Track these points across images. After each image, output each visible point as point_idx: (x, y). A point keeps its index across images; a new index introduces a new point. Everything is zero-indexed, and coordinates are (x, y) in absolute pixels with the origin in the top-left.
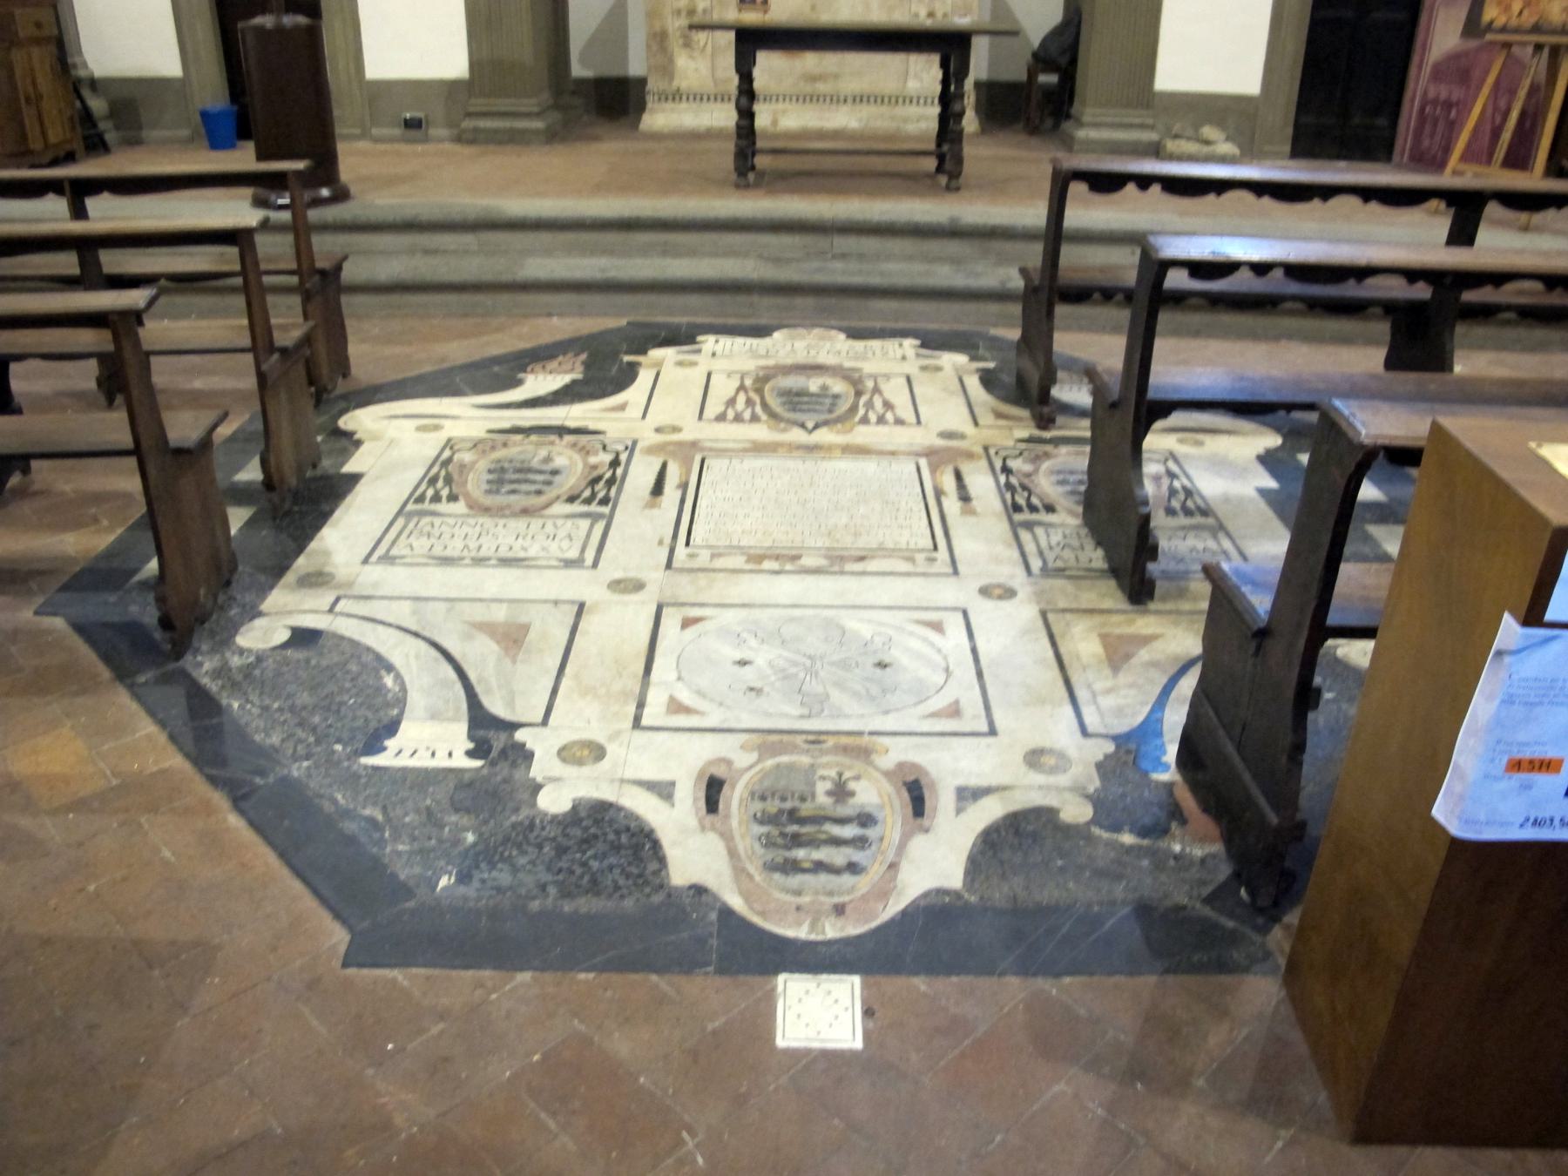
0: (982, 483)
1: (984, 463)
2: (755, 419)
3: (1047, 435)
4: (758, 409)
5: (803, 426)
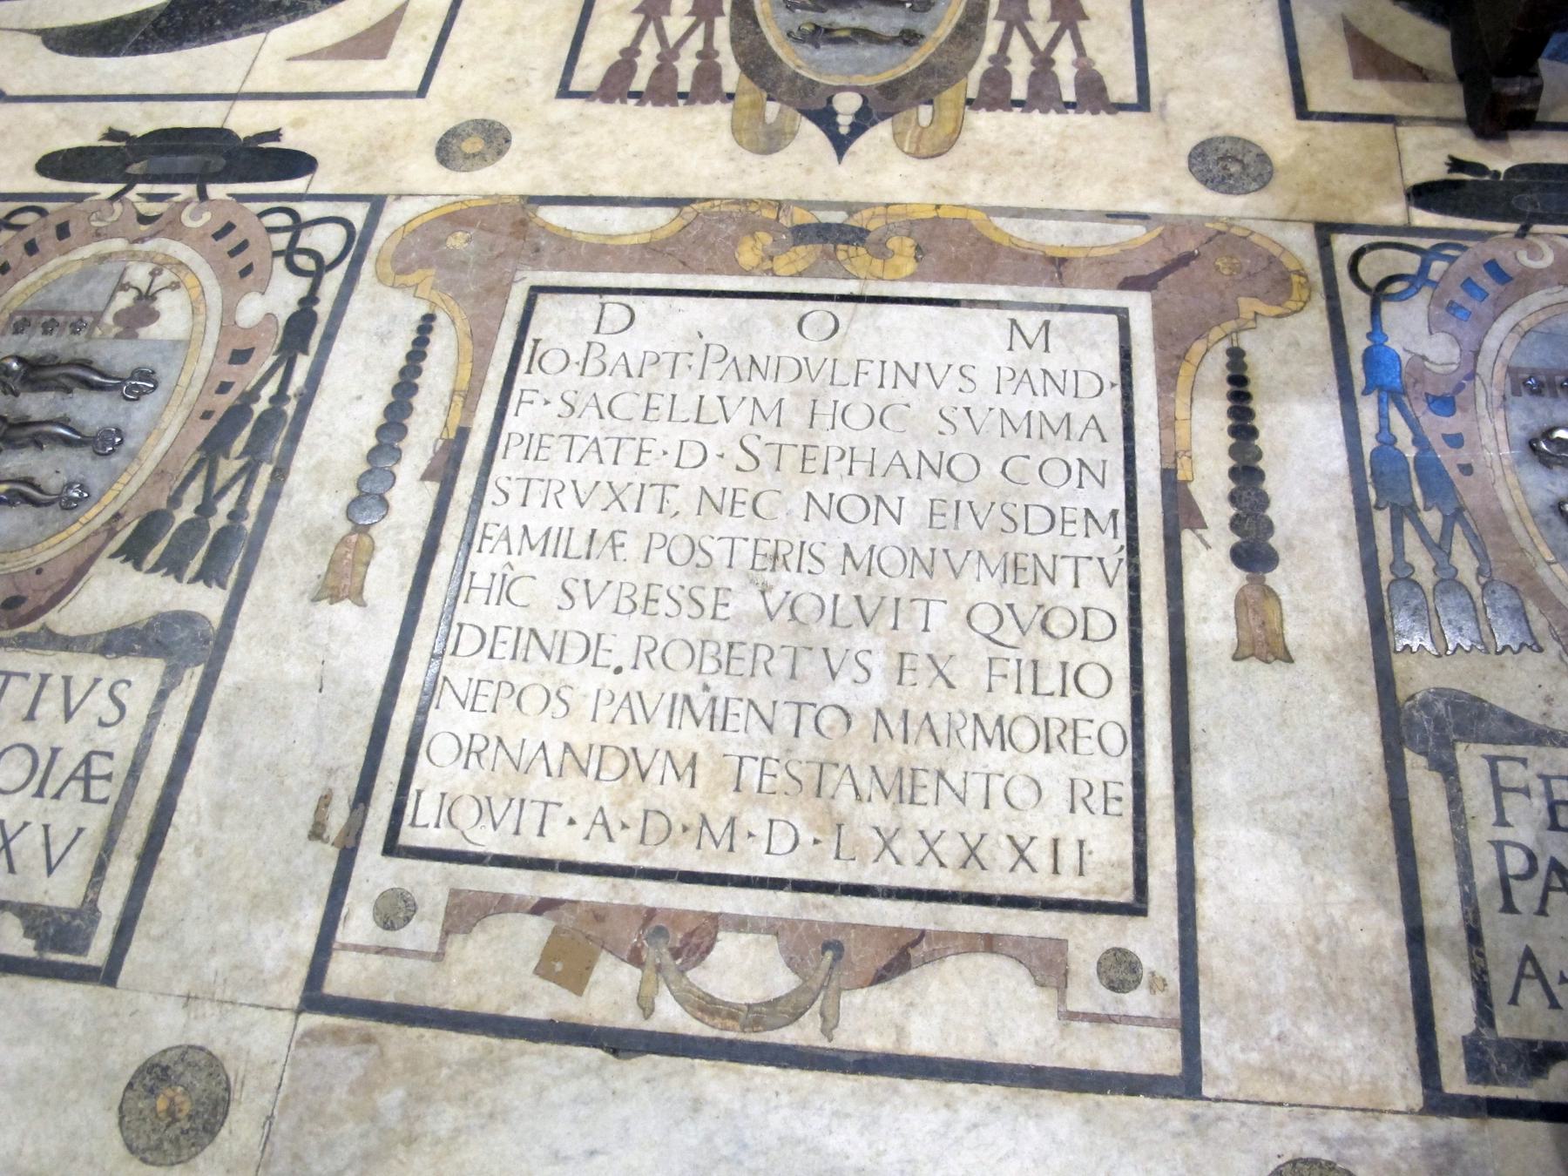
0: (1307, 444)
1: (1314, 320)
2: (707, 86)
3: (1499, 159)
4: (722, 26)
5: (824, 118)
